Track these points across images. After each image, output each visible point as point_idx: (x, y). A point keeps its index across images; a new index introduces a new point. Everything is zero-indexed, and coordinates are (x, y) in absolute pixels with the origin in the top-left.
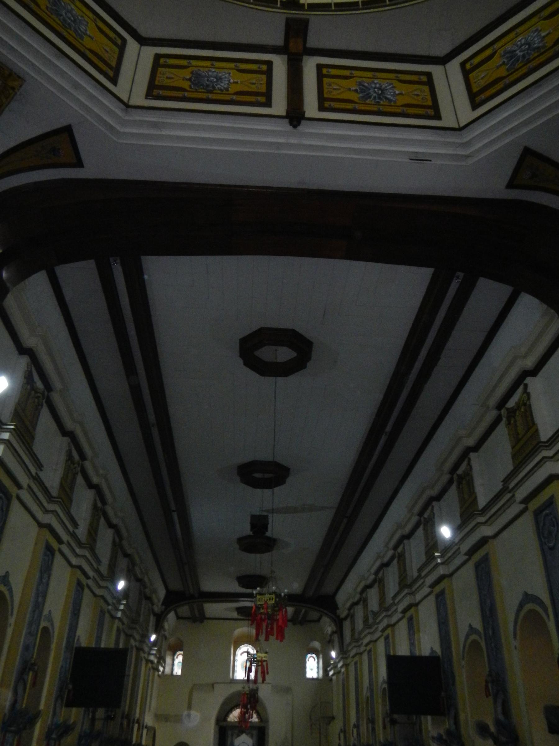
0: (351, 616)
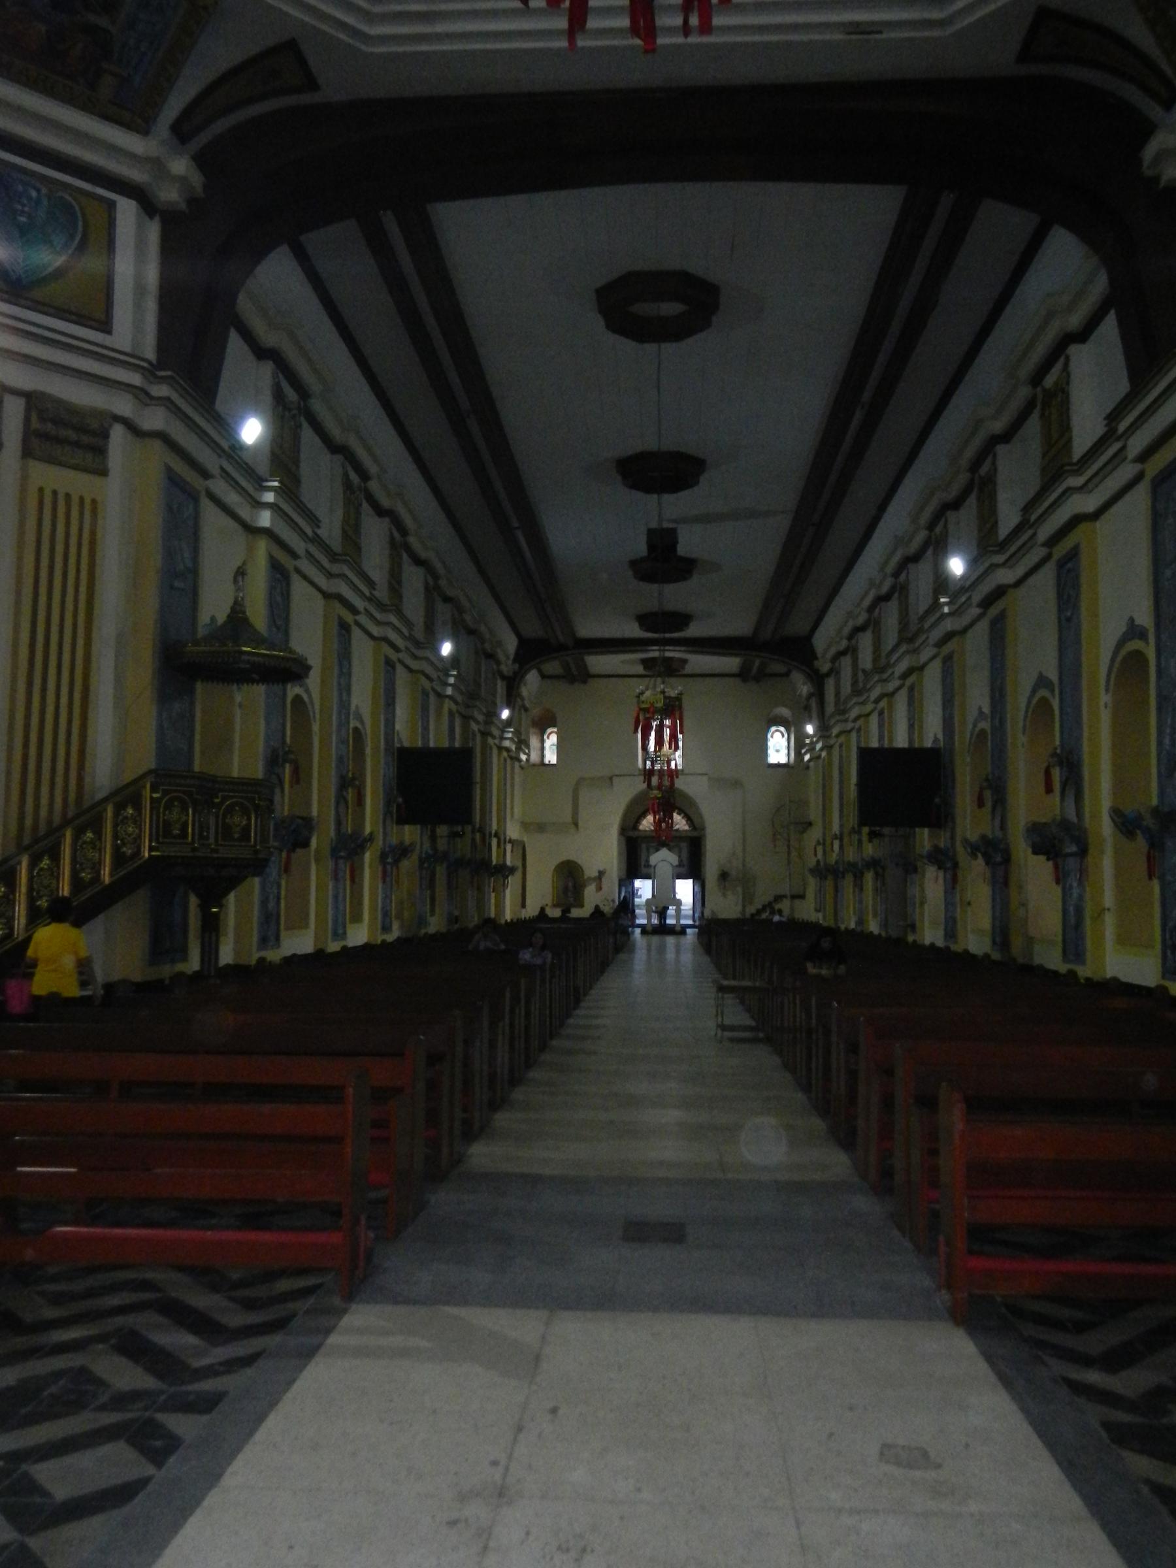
0: (834, 672)
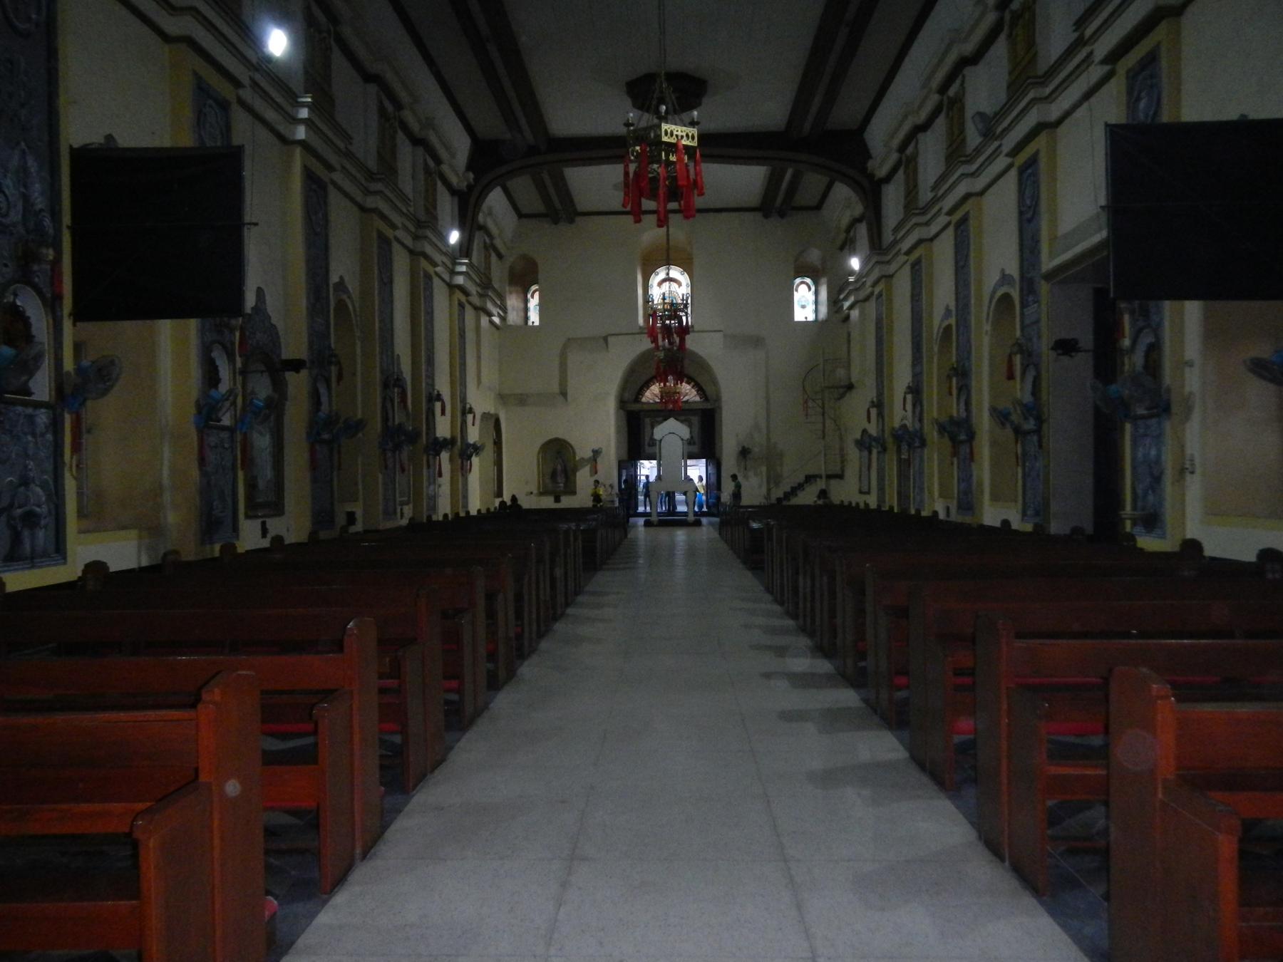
0: (907, 162)
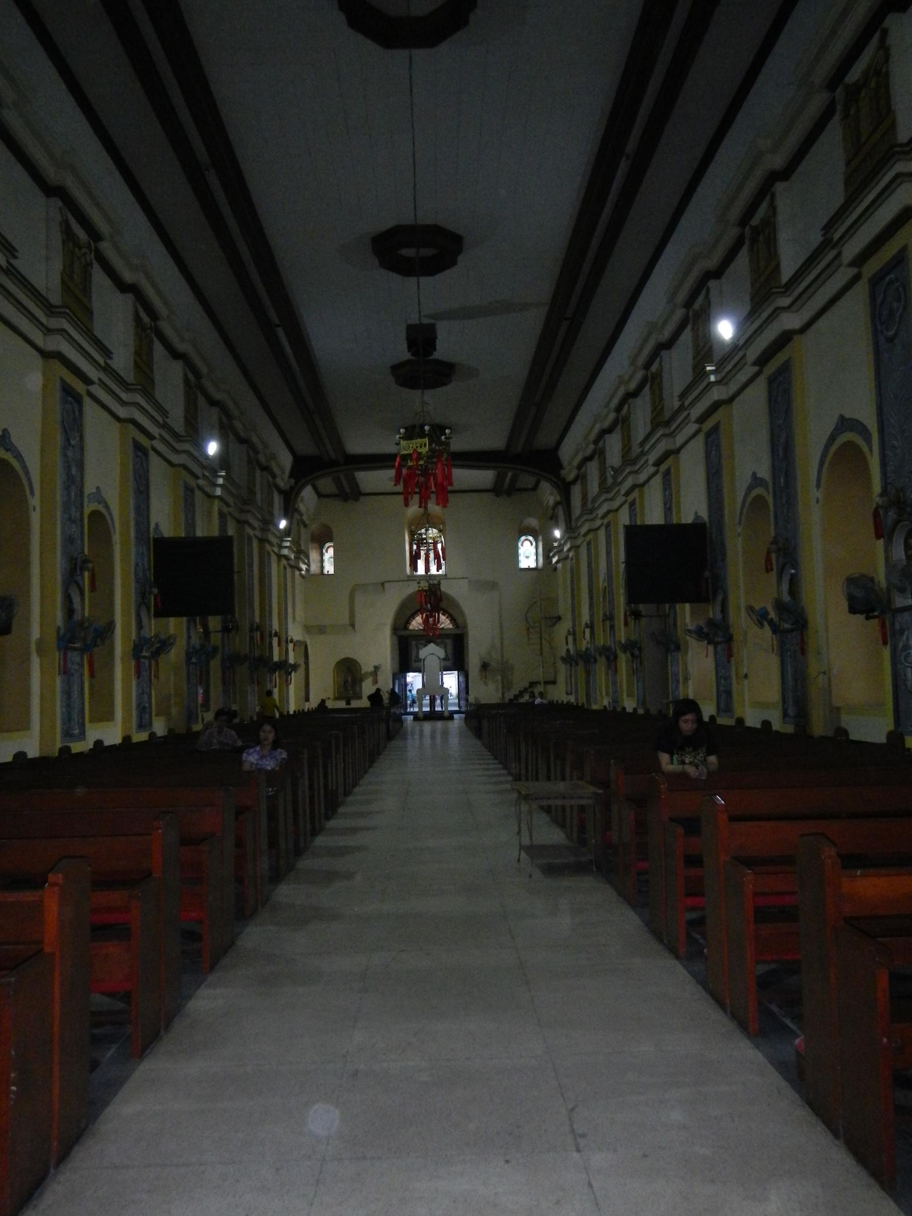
0: (581, 478)
